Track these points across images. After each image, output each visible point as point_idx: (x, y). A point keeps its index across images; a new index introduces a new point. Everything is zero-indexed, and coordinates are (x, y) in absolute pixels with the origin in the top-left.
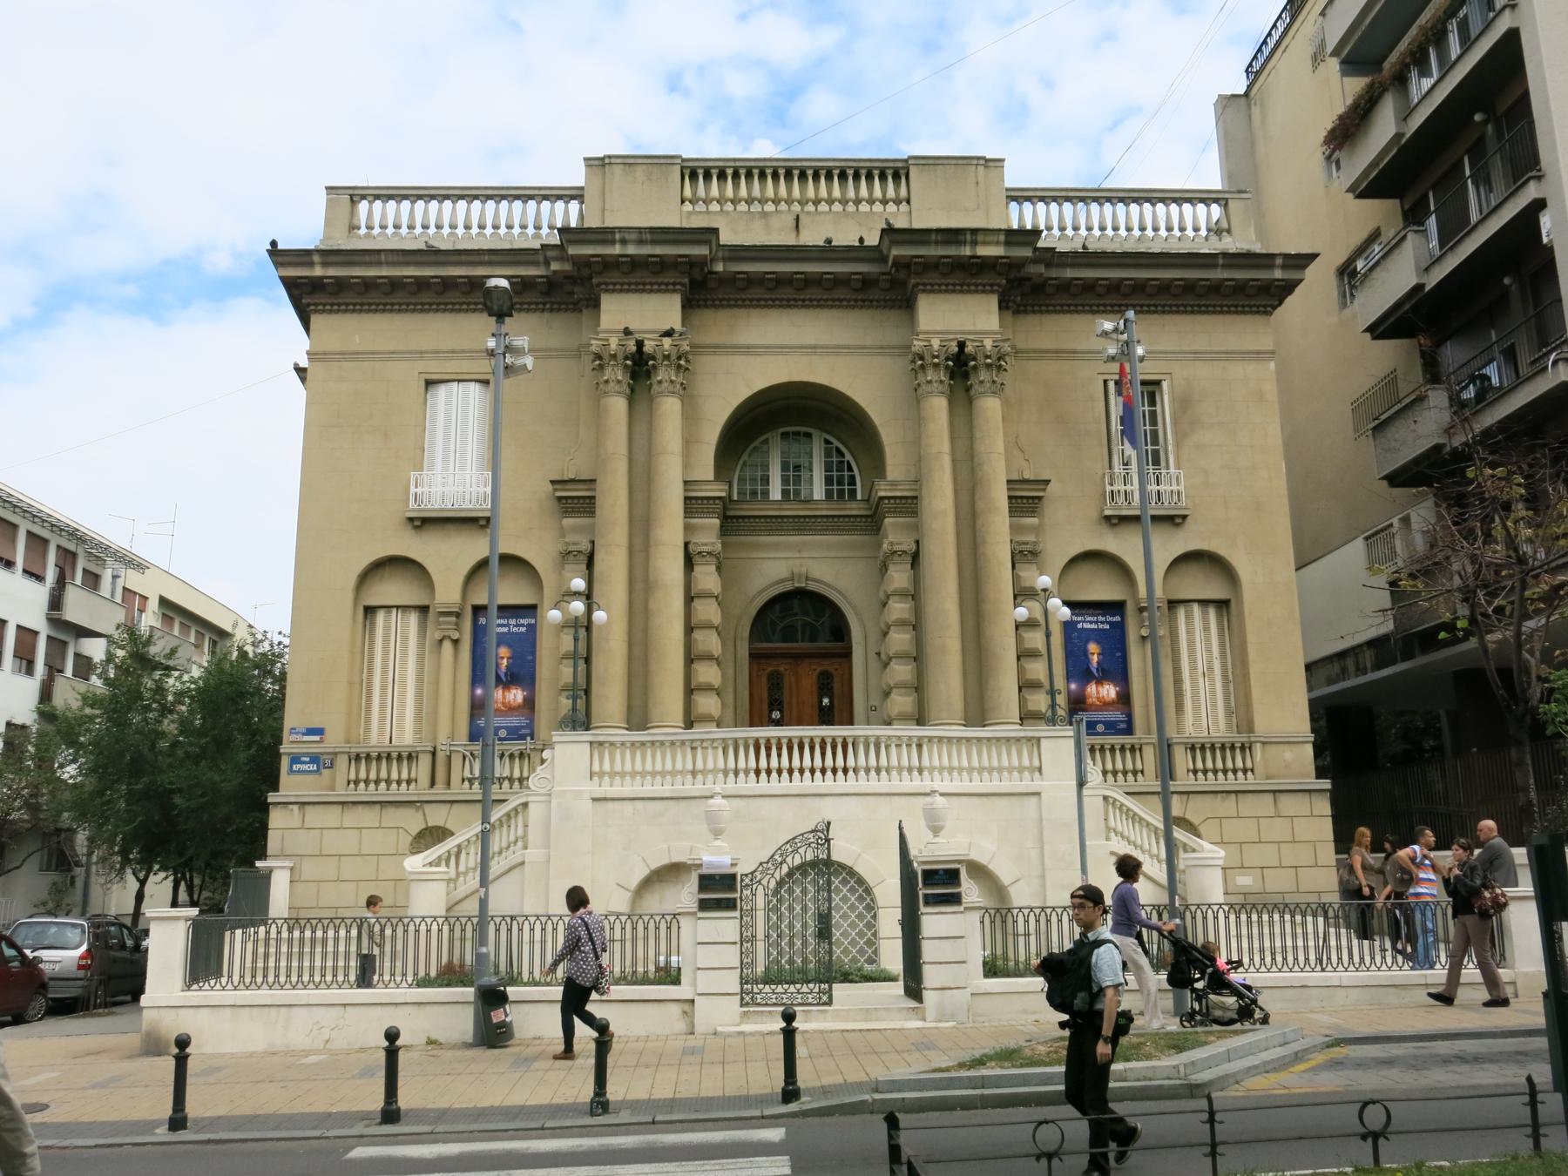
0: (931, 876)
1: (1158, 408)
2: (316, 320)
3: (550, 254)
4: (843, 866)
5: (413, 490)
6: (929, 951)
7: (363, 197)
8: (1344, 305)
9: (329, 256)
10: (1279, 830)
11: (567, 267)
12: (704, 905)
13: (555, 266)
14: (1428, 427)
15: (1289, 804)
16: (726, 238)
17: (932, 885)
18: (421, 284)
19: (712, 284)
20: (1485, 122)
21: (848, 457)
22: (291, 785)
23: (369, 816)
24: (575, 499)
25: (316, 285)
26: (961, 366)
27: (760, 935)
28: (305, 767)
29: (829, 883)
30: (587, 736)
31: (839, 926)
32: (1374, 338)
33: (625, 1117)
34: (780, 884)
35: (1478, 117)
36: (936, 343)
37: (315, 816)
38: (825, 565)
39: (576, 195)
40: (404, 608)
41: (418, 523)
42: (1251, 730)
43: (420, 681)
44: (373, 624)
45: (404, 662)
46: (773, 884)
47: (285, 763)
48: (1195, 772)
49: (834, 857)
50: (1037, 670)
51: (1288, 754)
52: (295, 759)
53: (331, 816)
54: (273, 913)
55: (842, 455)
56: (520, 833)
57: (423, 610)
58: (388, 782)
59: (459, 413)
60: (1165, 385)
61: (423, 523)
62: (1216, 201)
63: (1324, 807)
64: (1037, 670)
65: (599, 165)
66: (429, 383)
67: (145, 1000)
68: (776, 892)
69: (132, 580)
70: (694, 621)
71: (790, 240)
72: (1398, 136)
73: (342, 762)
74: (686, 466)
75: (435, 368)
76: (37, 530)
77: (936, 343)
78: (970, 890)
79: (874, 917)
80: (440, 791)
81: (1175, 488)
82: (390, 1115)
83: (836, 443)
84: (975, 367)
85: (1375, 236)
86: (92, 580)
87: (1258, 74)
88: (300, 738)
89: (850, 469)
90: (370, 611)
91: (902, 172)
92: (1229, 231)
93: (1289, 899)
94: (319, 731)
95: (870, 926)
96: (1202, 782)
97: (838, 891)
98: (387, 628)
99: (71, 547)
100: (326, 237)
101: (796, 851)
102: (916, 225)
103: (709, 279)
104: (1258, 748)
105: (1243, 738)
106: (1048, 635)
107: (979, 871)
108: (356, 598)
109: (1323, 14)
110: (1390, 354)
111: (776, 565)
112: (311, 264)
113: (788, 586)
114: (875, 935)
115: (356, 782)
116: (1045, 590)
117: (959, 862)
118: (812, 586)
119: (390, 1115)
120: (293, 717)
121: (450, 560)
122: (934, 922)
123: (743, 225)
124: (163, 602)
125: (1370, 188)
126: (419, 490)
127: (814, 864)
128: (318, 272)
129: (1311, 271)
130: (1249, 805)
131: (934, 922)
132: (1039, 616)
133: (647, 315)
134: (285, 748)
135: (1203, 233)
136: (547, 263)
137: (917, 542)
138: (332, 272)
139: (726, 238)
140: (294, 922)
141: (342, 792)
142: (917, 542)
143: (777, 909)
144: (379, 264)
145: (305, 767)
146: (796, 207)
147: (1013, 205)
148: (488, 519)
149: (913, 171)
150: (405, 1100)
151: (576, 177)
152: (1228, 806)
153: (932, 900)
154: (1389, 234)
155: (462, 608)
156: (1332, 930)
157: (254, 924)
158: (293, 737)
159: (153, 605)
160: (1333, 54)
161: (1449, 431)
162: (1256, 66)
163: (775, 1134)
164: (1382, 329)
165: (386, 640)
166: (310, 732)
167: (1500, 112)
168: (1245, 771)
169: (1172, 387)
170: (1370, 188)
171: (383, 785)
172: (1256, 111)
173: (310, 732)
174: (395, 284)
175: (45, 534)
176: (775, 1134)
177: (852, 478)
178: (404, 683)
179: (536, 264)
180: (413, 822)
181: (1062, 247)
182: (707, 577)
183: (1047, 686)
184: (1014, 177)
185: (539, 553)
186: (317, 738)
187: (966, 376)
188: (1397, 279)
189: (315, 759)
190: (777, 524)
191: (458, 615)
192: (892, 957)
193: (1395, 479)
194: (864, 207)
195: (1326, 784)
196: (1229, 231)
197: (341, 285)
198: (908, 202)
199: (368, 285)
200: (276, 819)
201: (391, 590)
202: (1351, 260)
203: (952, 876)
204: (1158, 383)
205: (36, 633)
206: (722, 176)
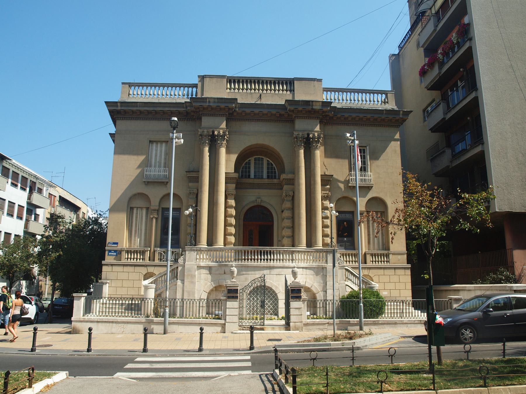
0: (293, 291)
1: (366, 154)
2: (118, 122)
3: (187, 104)
4: (269, 287)
5: (145, 173)
6: (292, 312)
7: (133, 86)
8: (425, 121)
9: (123, 103)
10: (395, 279)
11: (193, 109)
12: (229, 297)
14: (445, 161)
15: (398, 272)
16: (239, 101)
17: (294, 293)
18: (149, 112)
19: (235, 114)
20: (464, 71)
22: (109, 259)
23: (131, 269)
25: (119, 112)
27: (244, 306)
28: (113, 254)
29: (264, 292)
31: (267, 304)
32: (432, 132)
33: (208, 352)
34: (251, 292)
36: (301, 133)
37: (115, 268)
38: (267, 198)
39: (195, 86)
40: (141, 208)
42: (389, 249)
43: (146, 230)
44: (133, 212)
45: (142, 224)
46: (248, 292)
47: (107, 252)
48: (372, 262)
49: (267, 284)
50: (328, 231)
51: (399, 257)
52: (110, 251)
53: (120, 269)
54: (104, 295)
55: (272, 165)
57: (148, 209)
58: (137, 259)
60: (368, 147)
61: (148, 183)
62: (384, 93)
63: (409, 272)
64: (328, 231)
65: (202, 78)
66: (151, 142)
67: (73, 319)
68: (249, 294)
69: (52, 191)
70: (227, 215)
71: (259, 102)
73: (124, 253)
74: (226, 168)
75: (153, 138)
76: (24, 175)
77: (301, 133)
78: (304, 295)
79: (278, 302)
80: (152, 263)
81: (370, 178)
82: (145, 350)
83: (271, 161)
84: (312, 141)
85: (433, 101)
86: (40, 191)
87: (402, 48)
88: (111, 245)
89: (275, 169)
90: (132, 209)
91: (292, 82)
92: (387, 102)
93: (397, 299)
94: (117, 243)
95: (276, 304)
96: (374, 265)
97: (267, 294)
98: (137, 214)
99: (35, 181)
100: (121, 97)
101: (255, 283)
102: (296, 99)
104: (391, 256)
105: (385, 252)
106: (331, 221)
107: (308, 290)
108: (128, 205)
109: (419, 35)
110: (435, 137)
111: (252, 197)
113: (255, 204)
114: (278, 307)
115: (128, 259)
116: (331, 208)
117: (302, 287)
118: (263, 204)
119: (145, 350)
120: (109, 239)
121: (155, 195)
122: (294, 304)
123: (245, 97)
124: (60, 197)
125: (432, 87)
126: (147, 173)
127: (261, 286)
128: (119, 108)
129: (411, 116)
130: (387, 272)
131: (294, 304)
132: (329, 215)
134: (107, 248)
135: (380, 103)
136: (186, 107)
137: (294, 192)
138: (123, 108)
139: (239, 101)
140: (110, 298)
141: (124, 261)
142: (294, 192)
143: (249, 299)
144: (137, 106)
145: (113, 254)
146: (261, 91)
147: (325, 92)
148: (167, 182)
149: (295, 82)
150: (149, 347)
151: (196, 81)
152: (381, 272)
153: (293, 297)
154: (437, 100)
155: (159, 209)
156: (407, 307)
157: (99, 298)
158: (109, 245)
159: (58, 198)
160: (422, 47)
161: (451, 162)
162: (401, 46)
163: (248, 357)
164: (434, 130)
165: (137, 217)
166: (114, 243)
168: (387, 262)
169: (369, 148)
170: (432, 87)
171: (135, 260)
172: (401, 59)
173: (114, 243)
174: (141, 112)
175: (27, 176)
176: (248, 357)
178: (141, 230)
179: (183, 107)
180: (144, 271)
181: (339, 106)
182: (232, 202)
183: (330, 236)
184: (325, 84)
186: (116, 245)
187: (309, 144)
188: (438, 116)
189: (115, 251)
190: (253, 186)
191: (158, 211)
192: (282, 312)
193: (437, 175)
194: (281, 92)
195: (409, 266)
196: (387, 102)
197: (125, 112)
198: (294, 91)
199: (133, 112)
200: (104, 268)
202: (427, 107)
203: (299, 291)
204: (366, 147)
205: (24, 207)
206: (239, 82)
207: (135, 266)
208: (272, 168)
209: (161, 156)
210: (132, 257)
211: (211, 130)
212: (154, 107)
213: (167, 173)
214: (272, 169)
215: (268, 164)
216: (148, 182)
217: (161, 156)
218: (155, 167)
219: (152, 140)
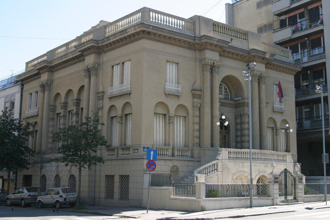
13: (197, 41)
20: (307, 40)
21: (228, 90)
24: (197, 93)
26: (260, 79)
30: (228, 149)
35: (306, 39)
41: (167, 95)
52: (144, 148)
56: (216, 168)
59: (171, 71)
61: (168, 95)
72: (291, 37)
103: (225, 51)
112: (149, 28)
133: (211, 56)
136: (195, 40)
149: (249, 34)
167: (310, 39)
177: (228, 95)
185: (189, 106)
201: (161, 110)
207: (165, 160)
208: (227, 91)
209: (172, 74)
210: (162, 153)
211: (213, 62)
212: (174, 35)
213: (180, 89)
214: (227, 93)
215: (225, 88)
216: (168, 94)
217: (172, 74)
218: (170, 82)
219: (168, 60)
